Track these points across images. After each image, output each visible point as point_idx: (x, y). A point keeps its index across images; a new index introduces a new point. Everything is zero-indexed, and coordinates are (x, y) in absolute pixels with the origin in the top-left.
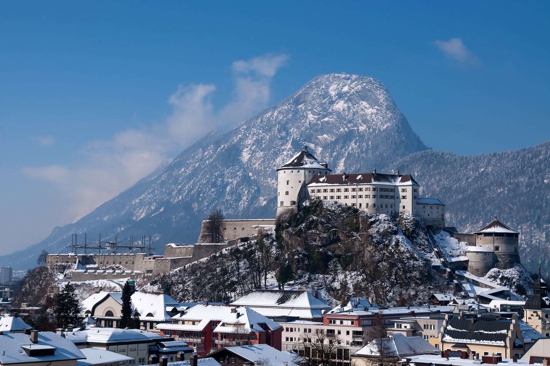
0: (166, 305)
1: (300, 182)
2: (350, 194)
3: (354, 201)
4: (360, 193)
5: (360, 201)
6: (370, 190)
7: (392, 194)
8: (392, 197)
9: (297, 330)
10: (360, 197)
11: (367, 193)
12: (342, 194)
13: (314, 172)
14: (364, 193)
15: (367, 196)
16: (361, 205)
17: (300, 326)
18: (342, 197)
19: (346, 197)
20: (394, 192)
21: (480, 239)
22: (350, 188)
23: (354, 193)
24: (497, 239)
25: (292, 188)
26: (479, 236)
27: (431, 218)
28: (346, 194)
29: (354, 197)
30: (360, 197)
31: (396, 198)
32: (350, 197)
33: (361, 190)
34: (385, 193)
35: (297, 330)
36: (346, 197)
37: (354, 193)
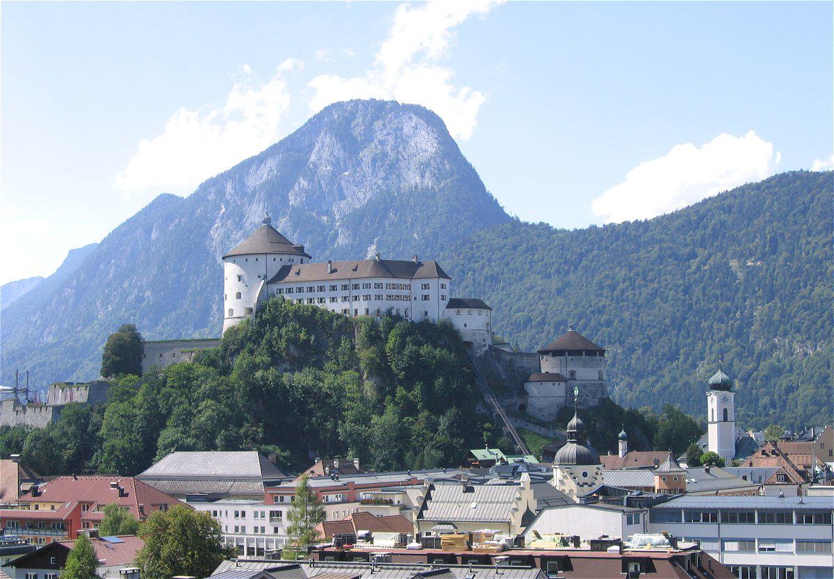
0: (21, 481)
3: (346, 305)
4: (355, 293)
5: (356, 305)
7: (405, 292)
9: (224, 513)
10: (356, 298)
13: (281, 259)
17: (228, 508)
28: (333, 294)
29: (345, 298)
31: (413, 299)
35: (224, 513)
36: (333, 299)
37: (346, 293)
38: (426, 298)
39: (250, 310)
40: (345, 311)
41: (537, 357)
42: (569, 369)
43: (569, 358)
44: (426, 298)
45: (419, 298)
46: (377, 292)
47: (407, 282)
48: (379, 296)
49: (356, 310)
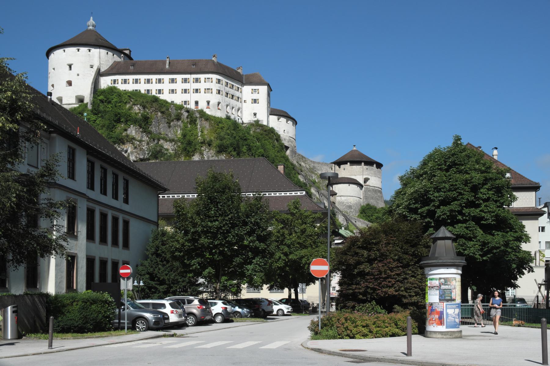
1: (92, 67)
2: (179, 86)
3: (186, 97)
4: (196, 86)
7: (237, 94)
8: (238, 98)
10: (197, 91)
11: (208, 85)
12: (166, 86)
14: (202, 86)
15: (208, 90)
16: (197, 103)
18: (166, 92)
19: (173, 91)
20: (241, 92)
25: (78, 75)
26: (342, 166)
27: (287, 136)
28: (173, 86)
29: (185, 91)
30: (197, 91)
32: (179, 91)
33: (197, 80)
34: (231, 92)
36: (173, 91)
37: (186, 86)
38: (255, 101)
40: (185, 102)
42: (365, 177)
44: (255, 101)
45: (249, 101)
49: (197, 103)
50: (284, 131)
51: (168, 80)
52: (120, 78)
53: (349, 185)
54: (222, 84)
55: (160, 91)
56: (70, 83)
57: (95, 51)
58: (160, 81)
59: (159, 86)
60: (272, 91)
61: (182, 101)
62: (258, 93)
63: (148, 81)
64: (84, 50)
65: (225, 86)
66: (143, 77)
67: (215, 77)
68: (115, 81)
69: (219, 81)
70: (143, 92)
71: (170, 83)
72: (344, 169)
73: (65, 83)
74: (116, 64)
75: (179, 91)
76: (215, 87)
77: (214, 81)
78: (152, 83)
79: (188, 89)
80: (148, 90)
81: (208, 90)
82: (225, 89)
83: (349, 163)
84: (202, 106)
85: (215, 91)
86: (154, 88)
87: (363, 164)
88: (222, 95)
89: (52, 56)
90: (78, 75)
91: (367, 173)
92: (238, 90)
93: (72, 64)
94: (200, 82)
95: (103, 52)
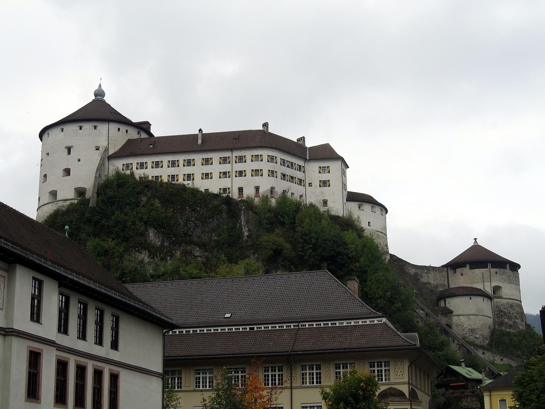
1: (97, 149)
2: (216, 168)
3: (225, 183)
4: (240, 167)
5: (238, 182)
6: (262, 160)
7: (299, 175)
10: (241, 173)
11: (256, 165)
12: (198, 170)
13: (127, 131)
14: (249, 166)
16: (241, 190)
19: (207, 176)
20: (304, 172)
21: (462, 275)
22: (216, 157)
23: (226, 168)
24: (496, 273)
25: (79, 160)
26: (459, 270)
28: (207, 169)
29: (225, 174)
30: (241, 173)
31: (307, 185)
32: (216, 175)
33: (241, 159)
34: (289, 172)
36: (207, 176)
37: (226, 168)
38: (325, 183)
39: (81, 192)
41: (445, 273)
42: (494, 284)
43: (493, 270)
45: (316, 183)
46: (271, 166)
47: (301, 163)
48: (273, 172)
49: (241, 190)
50: (369, 223)
51: (201, 160)
52: (134, 161)
53: (471, 298)
54: (276, 163)
55: (189, 177)
56: (67, 172)
57: (103, 128)
58: (189, 163)
59: (188, 170)
60: (349, 168)
61: (220, 189)
62: (329, 172)
63: (173, 164)
64: (88, 127)
65: (281, 164)
66: (165, 159)
67: (265, 153)
68: (128, 166)
69: (272, 159)
70: (165, 180)
71: (202, 164)
72: (462, 275)
73: (61, 173)
74: (130, 142)
75: (216, 175)
76: (265, 166)
77: (265, 158)
78: (178, 166)
79: (229, 172)
80: (173, 177)
81: (257, 172)
82: (280, 168)
83: (468, 266)
84: (249, 192)
85: (265, 173)
86: (181, 171)
87: (489, 265)
88: (277, 177)
89: (45, 137)
90: (79, 160)
91: (496, 279)
92: (300, 170)
93: (72, 147)
94: (245, 162)
95: (114, 127)
